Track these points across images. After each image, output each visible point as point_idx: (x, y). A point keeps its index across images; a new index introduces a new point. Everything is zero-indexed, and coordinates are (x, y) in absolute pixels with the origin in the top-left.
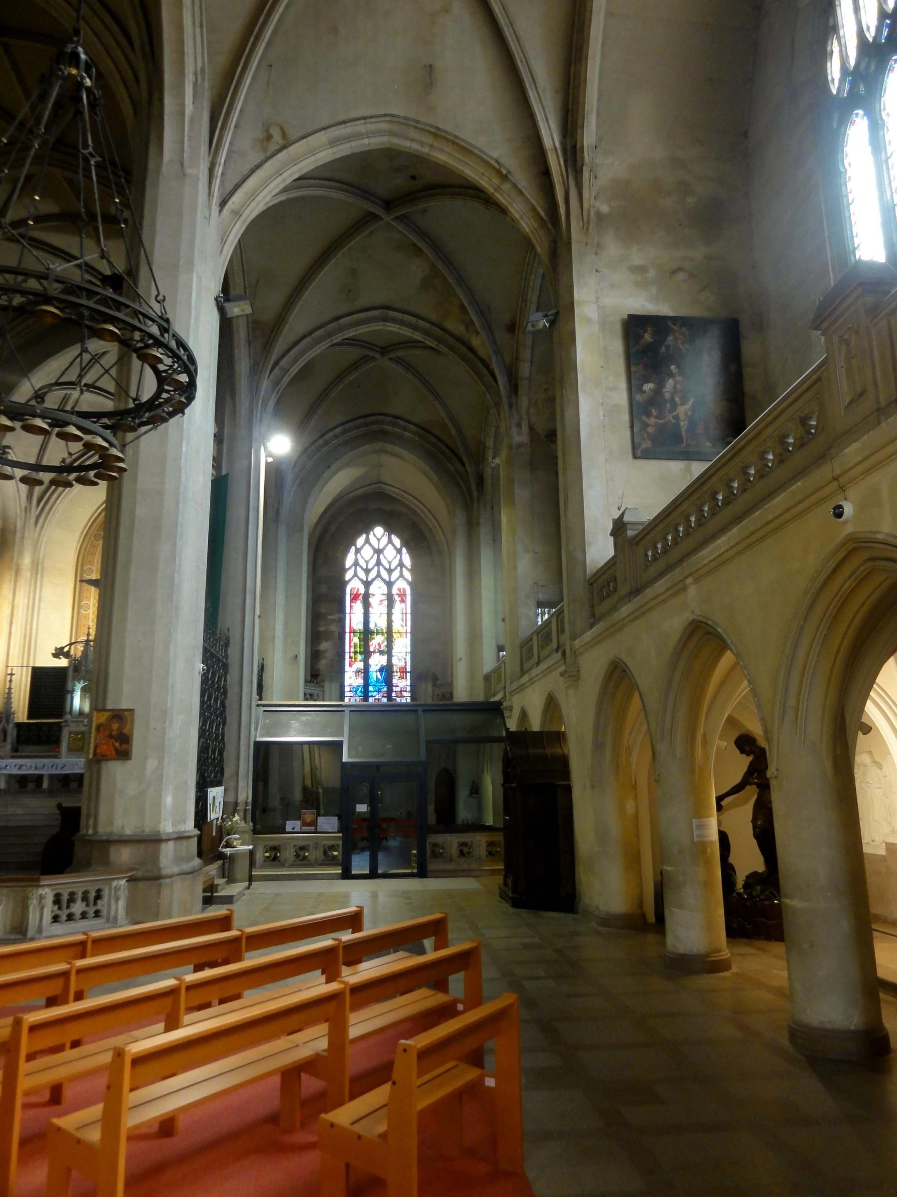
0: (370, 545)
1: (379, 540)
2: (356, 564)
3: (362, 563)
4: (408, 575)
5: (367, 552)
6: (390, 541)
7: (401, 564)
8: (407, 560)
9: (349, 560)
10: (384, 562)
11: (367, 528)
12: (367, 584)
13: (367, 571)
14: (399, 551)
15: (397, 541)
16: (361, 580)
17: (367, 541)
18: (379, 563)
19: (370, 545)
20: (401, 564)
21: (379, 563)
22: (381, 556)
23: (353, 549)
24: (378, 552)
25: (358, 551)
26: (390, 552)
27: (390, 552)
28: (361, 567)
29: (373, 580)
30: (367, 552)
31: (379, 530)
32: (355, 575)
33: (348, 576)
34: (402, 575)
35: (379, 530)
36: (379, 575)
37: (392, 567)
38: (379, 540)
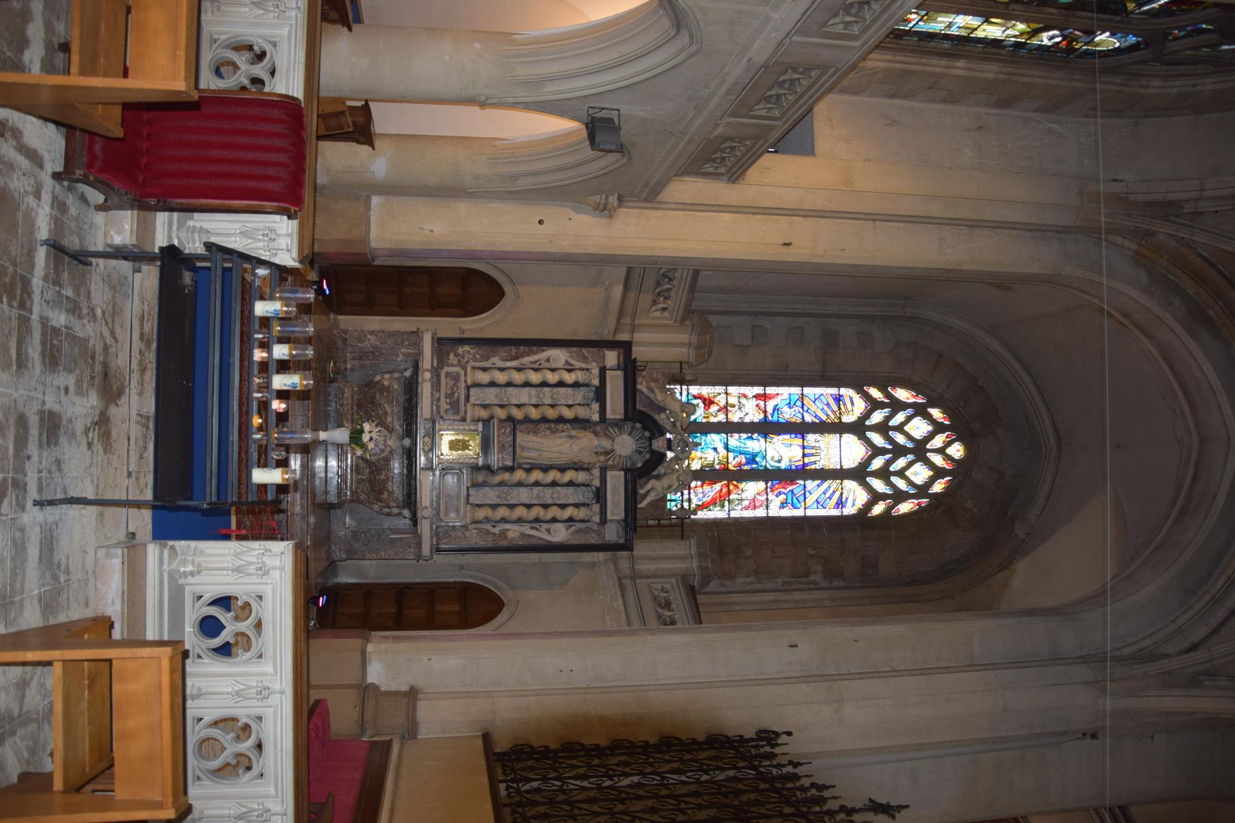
0: (930, 436)
1: (941, 451)
2: (897, 406)
3: (900, 417)
4: (878, 509)
5: (918, 428)
6: (938, 473)
7: (899, 496)
8: (905, 507)
9: (902, 394)
10: (901, 463)
11: (959, 429)
12: (858, 428)
13: (883, 428)
14: (922, 490)
15: (938, 487)
16: (867, 415)
17: (938, 428)
18: (899, 451)
19: (930, 436)
20: (899, 496)
21: (899, 451)
22: (910, 457)
23: (921, 400)
24: (919, 450)
25: (920, 411)
26: (920, 473)
27: (920, 473)
28: (888, 419)
29: (869, 442)
30: (918, 428)
31: (957, 451)
32: (874, 405)
33: (875, 393)
34: (876, 497)
35: (957, 451)
36: (877, 451)
37: (894, 479)
38: (941, 451)
